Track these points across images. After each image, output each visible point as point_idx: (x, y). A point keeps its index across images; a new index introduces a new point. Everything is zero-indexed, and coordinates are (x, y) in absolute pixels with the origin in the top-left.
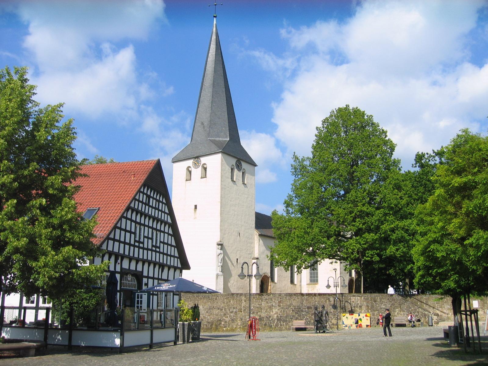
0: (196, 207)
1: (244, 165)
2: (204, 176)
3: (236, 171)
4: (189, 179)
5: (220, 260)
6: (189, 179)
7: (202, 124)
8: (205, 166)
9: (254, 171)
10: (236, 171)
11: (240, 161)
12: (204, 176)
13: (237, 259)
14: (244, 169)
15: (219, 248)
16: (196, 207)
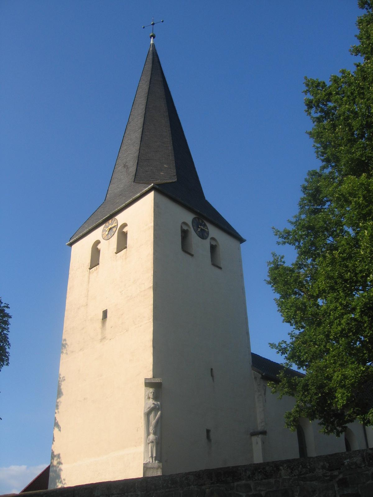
0: (105, 313)
1: (213, 231)
2: (122, 244)
3: (194, 237)
4: (95, 262)
5: (151, 430)
6: (95, 262)
7: (125, 166)
8: (125, 230)
9: (239, 249)
10: (194, 237)
11: (203, 222)
12: (122, 244)
13: (208, 431)
14: (213, 239)
15: (151, 396)
16: (105, 313)
